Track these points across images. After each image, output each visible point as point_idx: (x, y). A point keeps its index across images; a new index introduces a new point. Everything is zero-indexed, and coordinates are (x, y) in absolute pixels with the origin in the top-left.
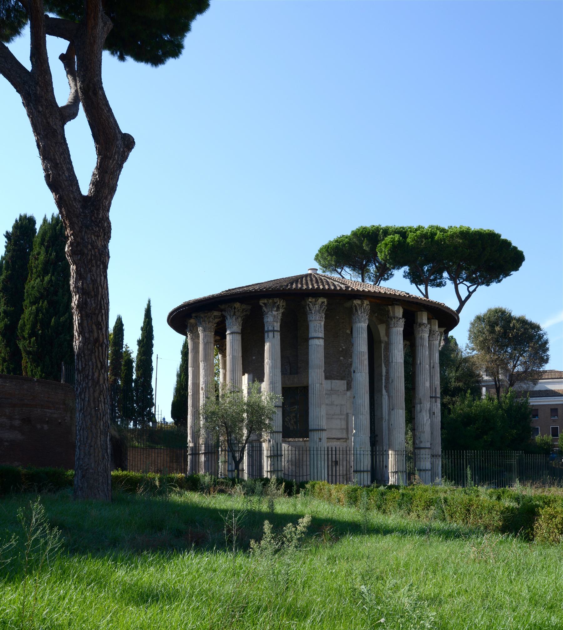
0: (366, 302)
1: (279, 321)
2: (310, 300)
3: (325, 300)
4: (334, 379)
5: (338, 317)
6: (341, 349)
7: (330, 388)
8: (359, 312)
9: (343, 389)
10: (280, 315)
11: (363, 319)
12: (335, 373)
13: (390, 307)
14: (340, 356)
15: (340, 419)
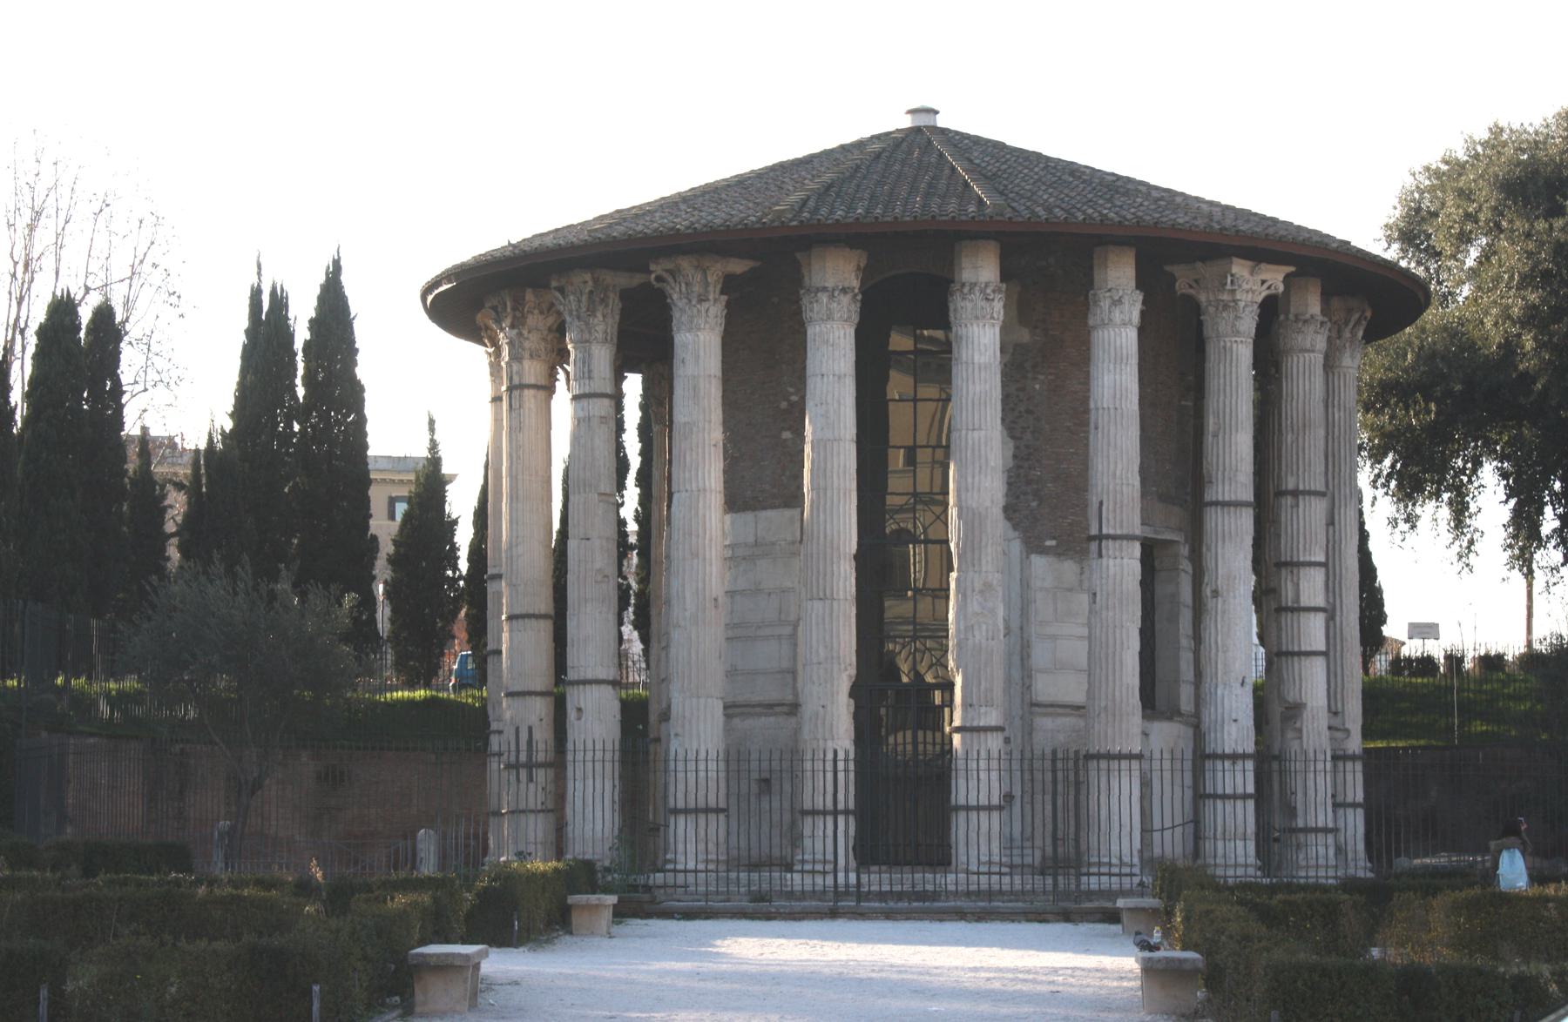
0: (685, 264)
1: (527, 355)
2: (554, 284)
3: (588, 277)
4: (765, 508)
5: (776, 300)
6: (784, 405)
7: (751, 539)
8: (675, 297)
9: (789, 538)
10: (534, 337)
11: (685, 319)
12: (767, 487)
13: (798, 255)
14: (783, 429)
15: (780, 637)
